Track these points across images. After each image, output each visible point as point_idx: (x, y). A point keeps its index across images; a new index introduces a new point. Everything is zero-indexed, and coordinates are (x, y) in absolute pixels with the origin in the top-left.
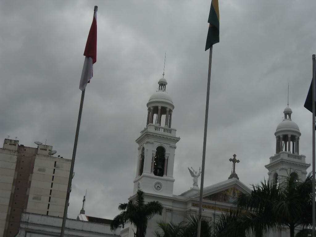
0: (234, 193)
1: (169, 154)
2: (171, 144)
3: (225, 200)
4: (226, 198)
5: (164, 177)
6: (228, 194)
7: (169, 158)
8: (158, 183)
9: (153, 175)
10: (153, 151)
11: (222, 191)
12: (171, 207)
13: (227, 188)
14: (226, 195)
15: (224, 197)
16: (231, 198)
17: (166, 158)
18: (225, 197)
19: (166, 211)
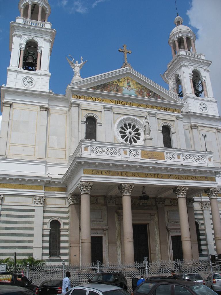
0: (128, 83)
1: (43, 47)
2: (44, 37)
3: (117, 91)
4: (118, 89)
5: (37, 72)
6: (121, 84)
7: (42, 52)
8: (29, 78)
9: (21, 69)
10: (20, 44)
11: (113, 82)
12: (48, 105)
13: (119, 78)
14: (118, 85)
15: (116, 88)
16: (124, 89)
17: (39, 52)
18: (117, 88)
19: (41, 110)
